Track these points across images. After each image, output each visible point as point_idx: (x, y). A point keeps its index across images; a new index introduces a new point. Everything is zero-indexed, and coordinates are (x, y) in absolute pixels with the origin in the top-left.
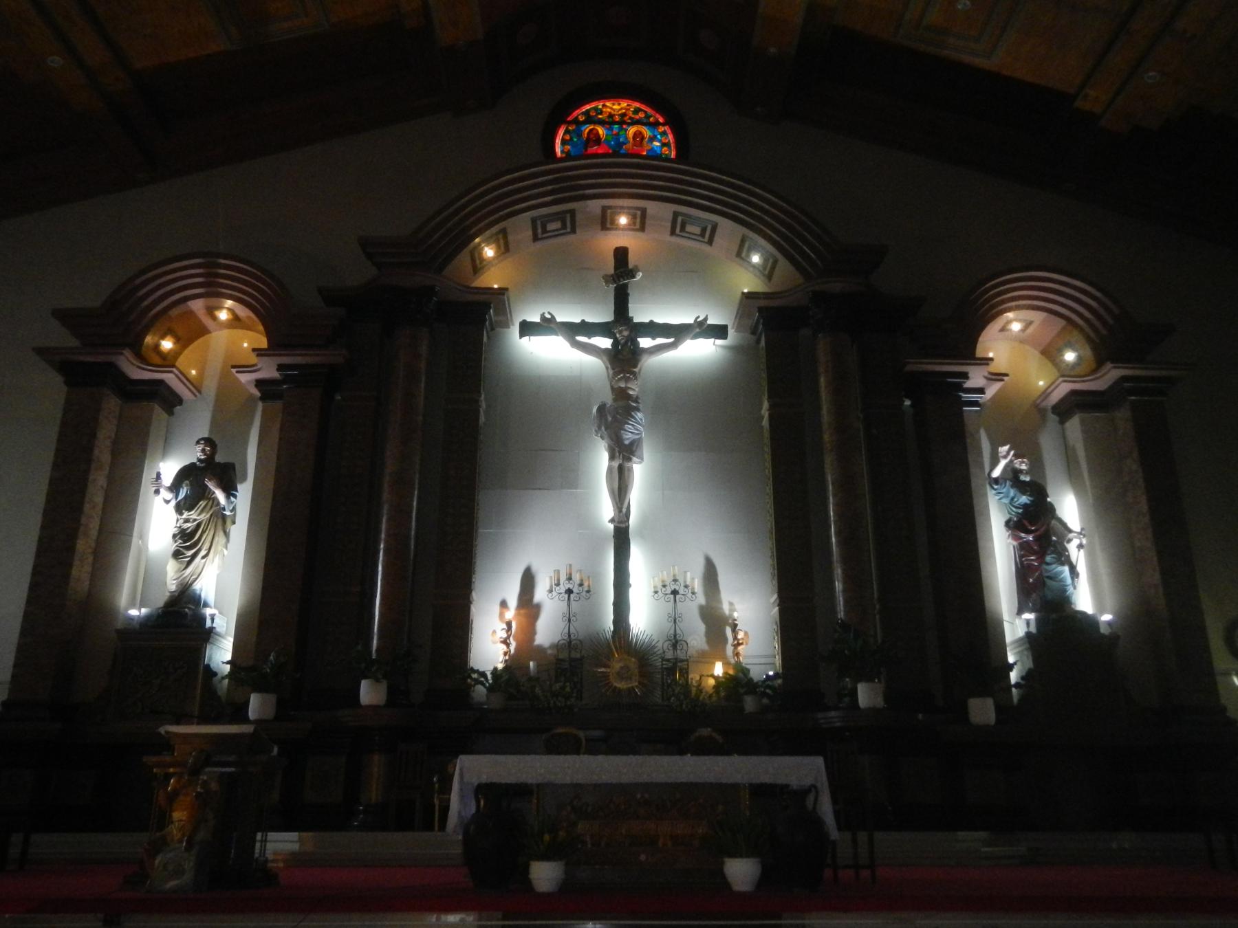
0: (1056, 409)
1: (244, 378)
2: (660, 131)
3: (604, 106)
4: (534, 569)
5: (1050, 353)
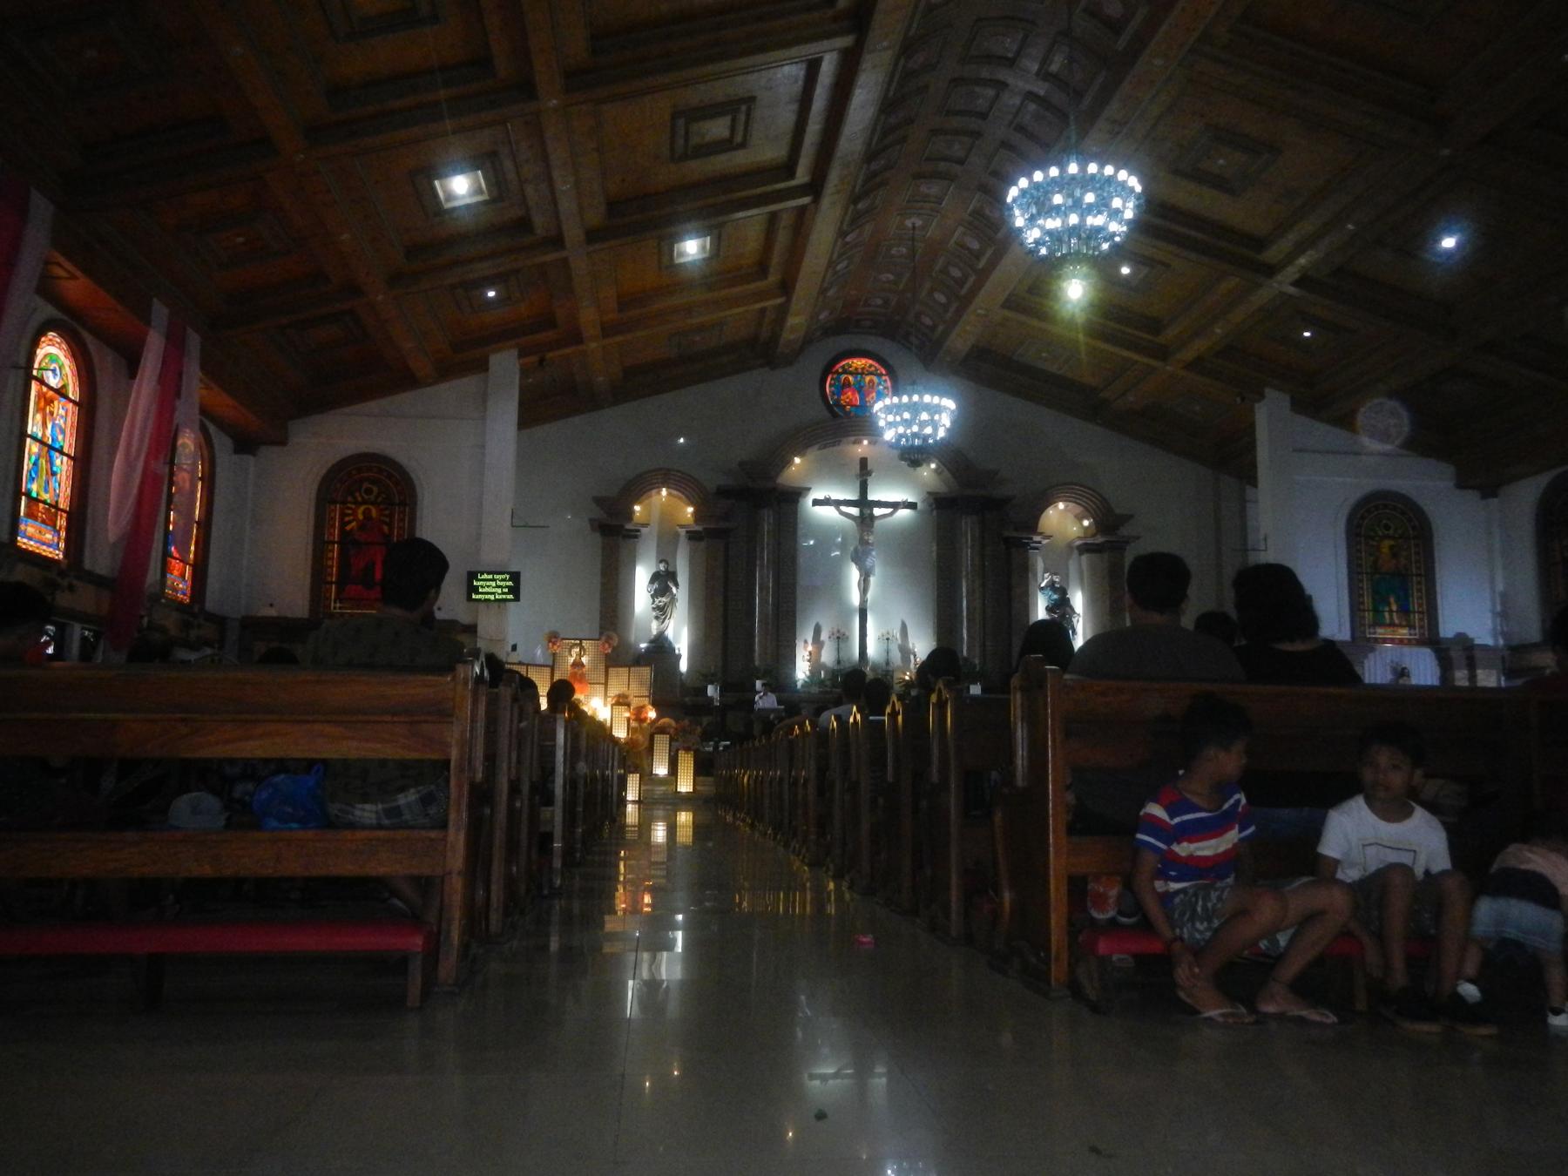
0: (1079, 548)
1: (680, 530)
4: (820, 623)
5: (1080, 518)
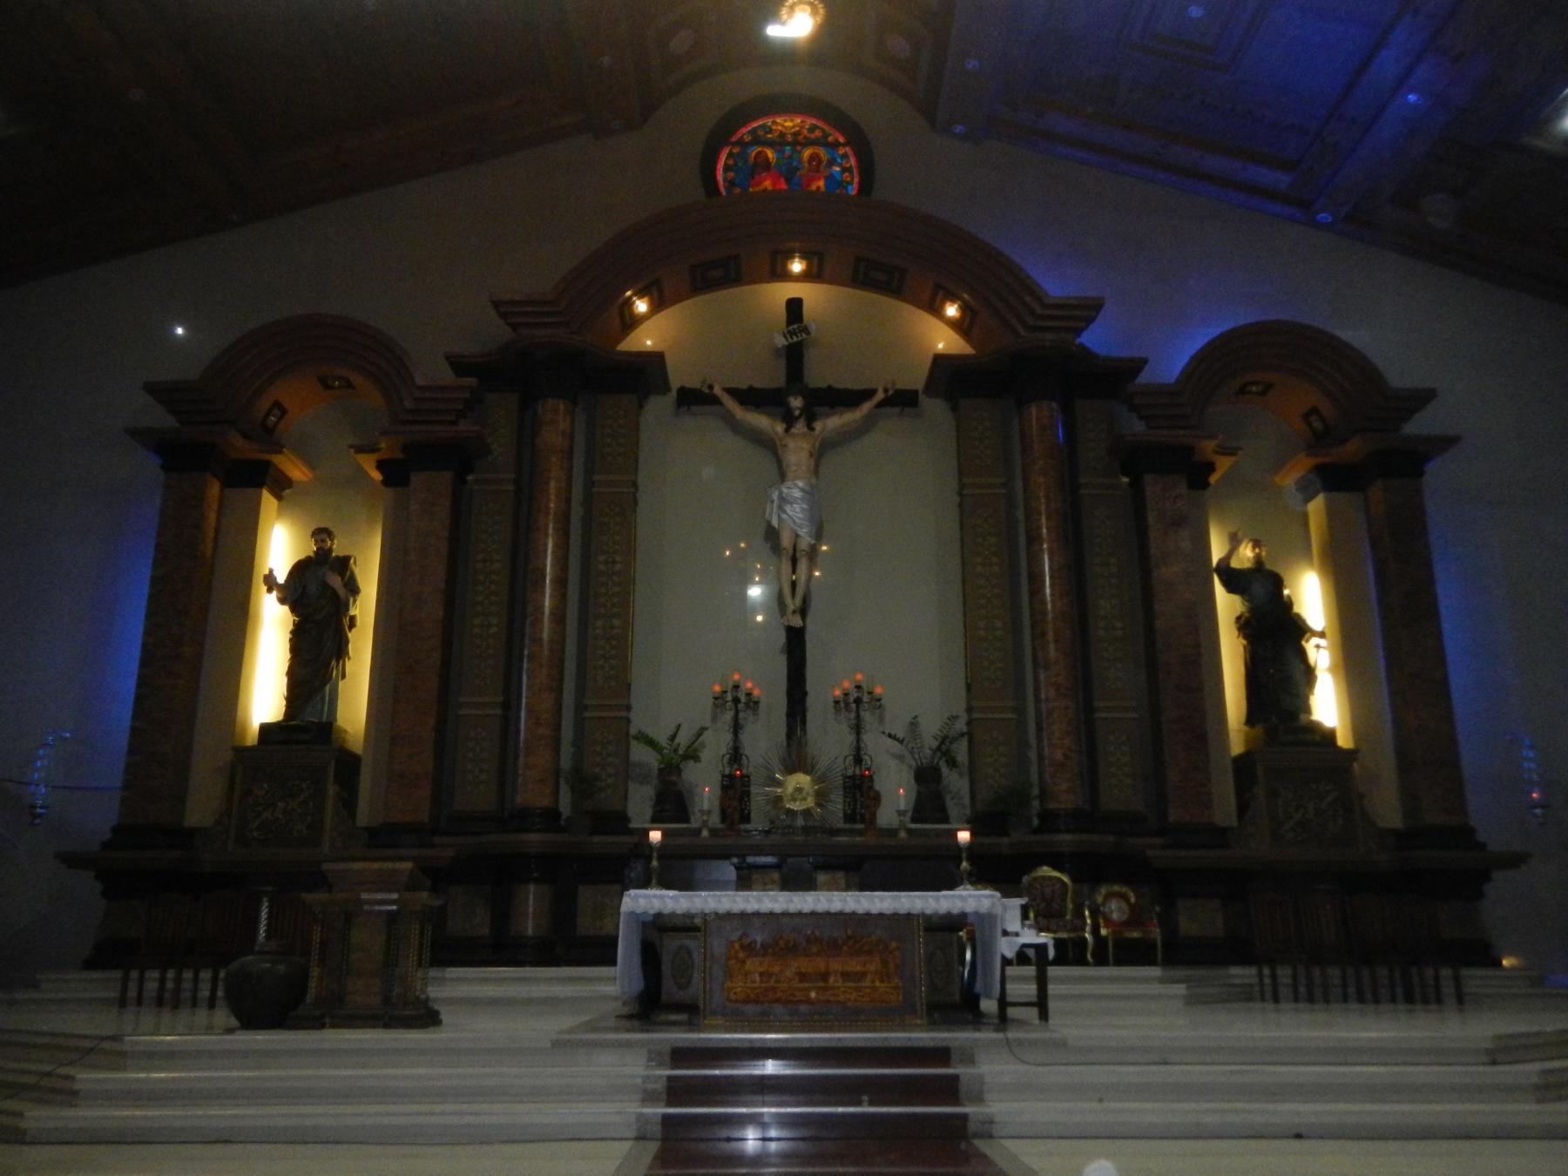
2: (840, 152)
3: (774, 123)
